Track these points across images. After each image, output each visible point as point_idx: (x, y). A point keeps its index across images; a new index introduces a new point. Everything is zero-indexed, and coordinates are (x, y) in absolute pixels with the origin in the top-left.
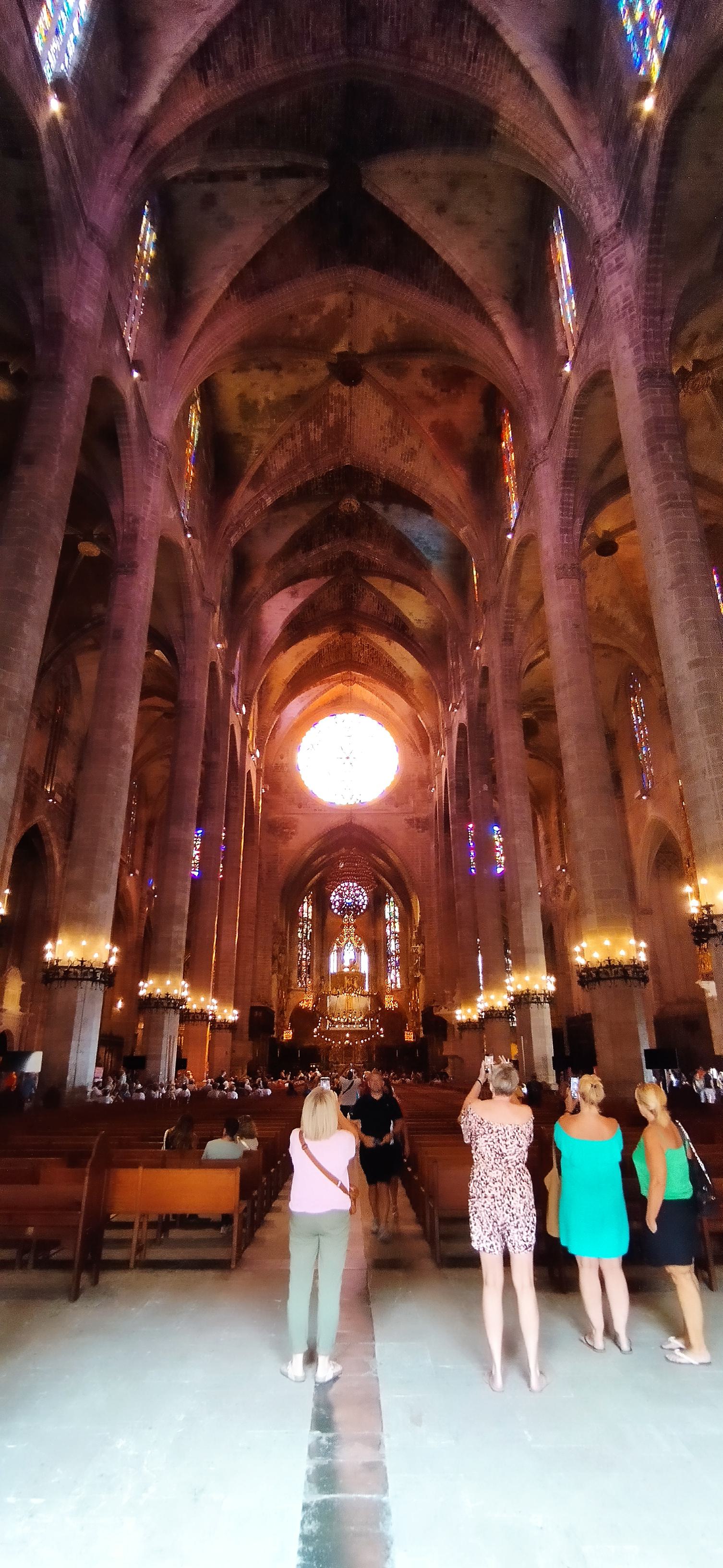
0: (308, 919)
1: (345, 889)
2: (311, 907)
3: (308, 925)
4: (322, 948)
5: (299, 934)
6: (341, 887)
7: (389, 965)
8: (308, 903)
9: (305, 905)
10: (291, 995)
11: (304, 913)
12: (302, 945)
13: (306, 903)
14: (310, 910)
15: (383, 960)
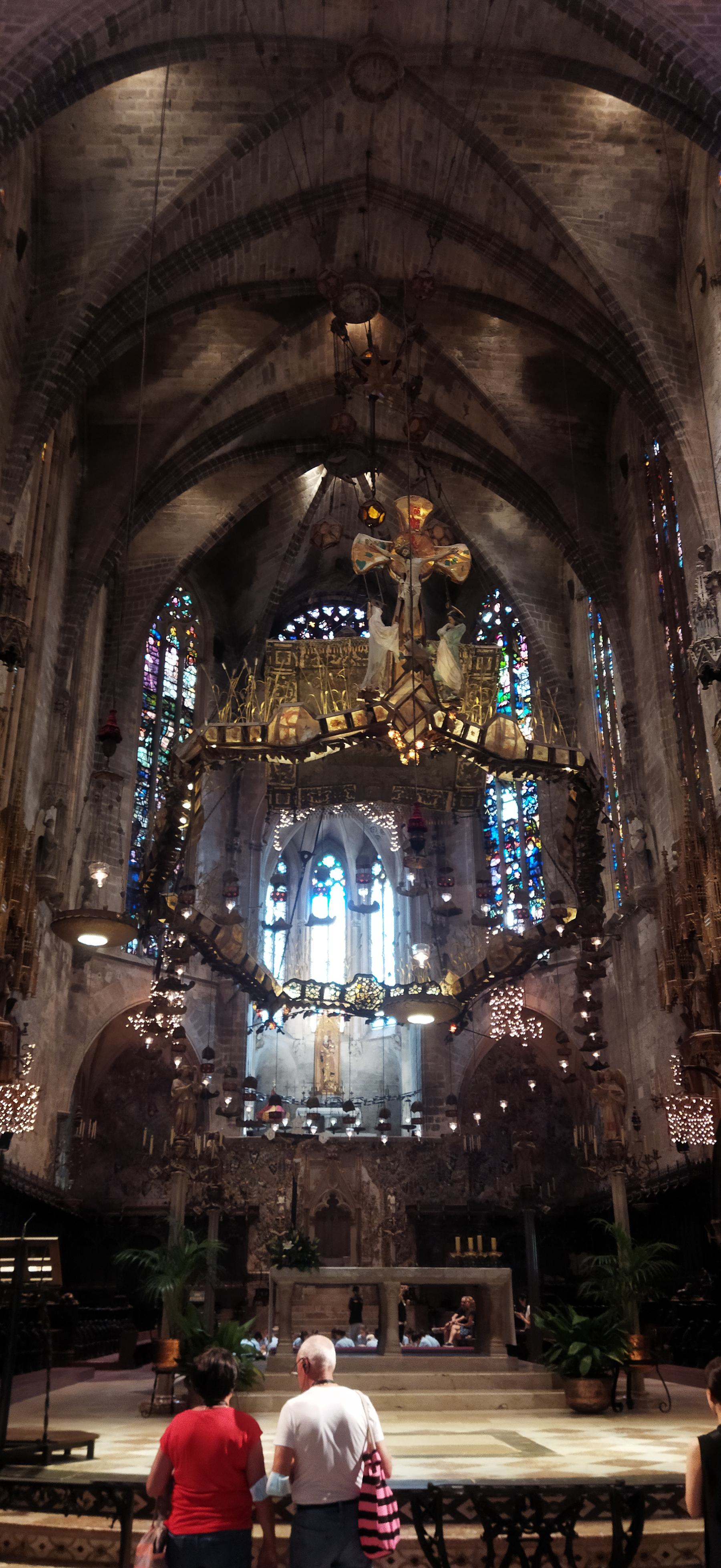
0: (176, 708)
1: (323, 626)
2: (194, 670)
3: (176, 727)
4: (234, 822)
5: (142, 752)
6: (309, 618)
7: (496, 878)
8: (182, 653)
9: (172, 658)
10: (92, 980)
11: (166, 683)
12: (150, 792)
13: (174, 650)
14: (190, 678)
15: (469, 861)
